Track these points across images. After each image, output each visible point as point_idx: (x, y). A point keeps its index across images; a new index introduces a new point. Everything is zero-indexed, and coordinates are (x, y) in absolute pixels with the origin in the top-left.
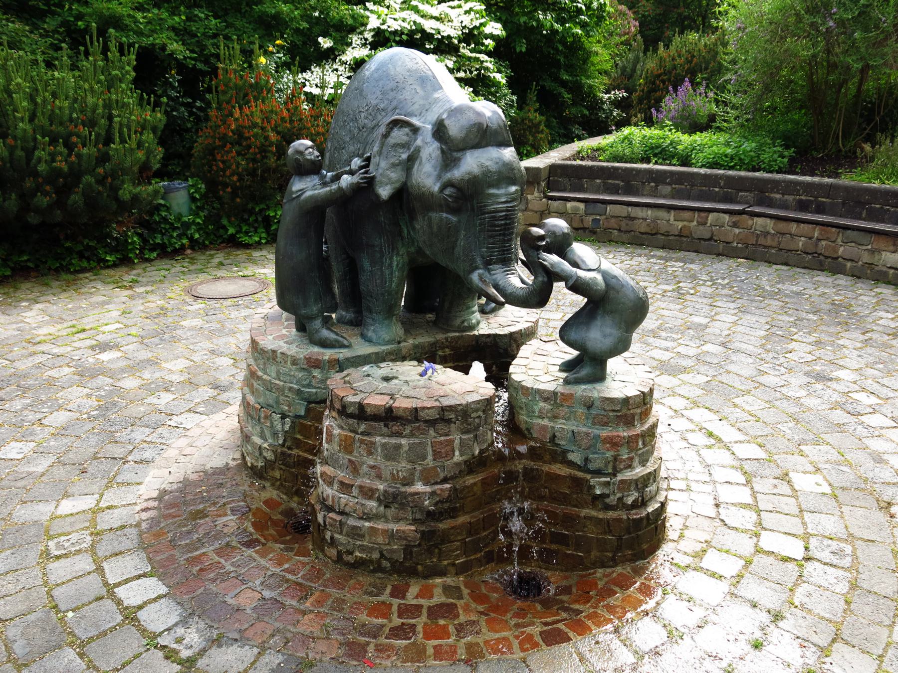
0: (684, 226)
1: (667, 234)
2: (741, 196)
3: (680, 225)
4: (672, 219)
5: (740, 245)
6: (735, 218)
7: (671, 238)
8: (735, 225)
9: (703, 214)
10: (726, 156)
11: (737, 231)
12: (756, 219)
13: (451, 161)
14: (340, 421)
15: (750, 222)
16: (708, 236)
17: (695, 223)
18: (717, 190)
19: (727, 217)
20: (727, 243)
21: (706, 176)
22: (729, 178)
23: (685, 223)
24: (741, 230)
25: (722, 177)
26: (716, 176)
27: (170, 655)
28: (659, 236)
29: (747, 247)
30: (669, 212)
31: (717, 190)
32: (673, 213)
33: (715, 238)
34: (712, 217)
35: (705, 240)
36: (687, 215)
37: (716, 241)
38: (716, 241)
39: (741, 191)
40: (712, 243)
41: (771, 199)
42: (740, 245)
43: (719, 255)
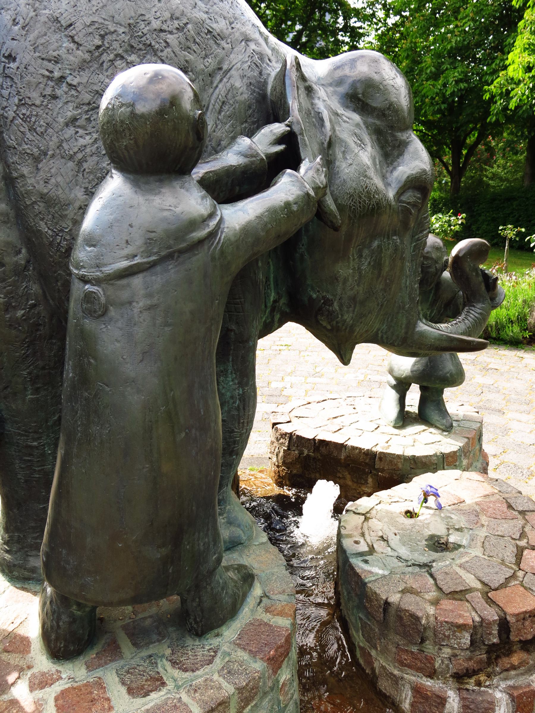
13: (394, 147)
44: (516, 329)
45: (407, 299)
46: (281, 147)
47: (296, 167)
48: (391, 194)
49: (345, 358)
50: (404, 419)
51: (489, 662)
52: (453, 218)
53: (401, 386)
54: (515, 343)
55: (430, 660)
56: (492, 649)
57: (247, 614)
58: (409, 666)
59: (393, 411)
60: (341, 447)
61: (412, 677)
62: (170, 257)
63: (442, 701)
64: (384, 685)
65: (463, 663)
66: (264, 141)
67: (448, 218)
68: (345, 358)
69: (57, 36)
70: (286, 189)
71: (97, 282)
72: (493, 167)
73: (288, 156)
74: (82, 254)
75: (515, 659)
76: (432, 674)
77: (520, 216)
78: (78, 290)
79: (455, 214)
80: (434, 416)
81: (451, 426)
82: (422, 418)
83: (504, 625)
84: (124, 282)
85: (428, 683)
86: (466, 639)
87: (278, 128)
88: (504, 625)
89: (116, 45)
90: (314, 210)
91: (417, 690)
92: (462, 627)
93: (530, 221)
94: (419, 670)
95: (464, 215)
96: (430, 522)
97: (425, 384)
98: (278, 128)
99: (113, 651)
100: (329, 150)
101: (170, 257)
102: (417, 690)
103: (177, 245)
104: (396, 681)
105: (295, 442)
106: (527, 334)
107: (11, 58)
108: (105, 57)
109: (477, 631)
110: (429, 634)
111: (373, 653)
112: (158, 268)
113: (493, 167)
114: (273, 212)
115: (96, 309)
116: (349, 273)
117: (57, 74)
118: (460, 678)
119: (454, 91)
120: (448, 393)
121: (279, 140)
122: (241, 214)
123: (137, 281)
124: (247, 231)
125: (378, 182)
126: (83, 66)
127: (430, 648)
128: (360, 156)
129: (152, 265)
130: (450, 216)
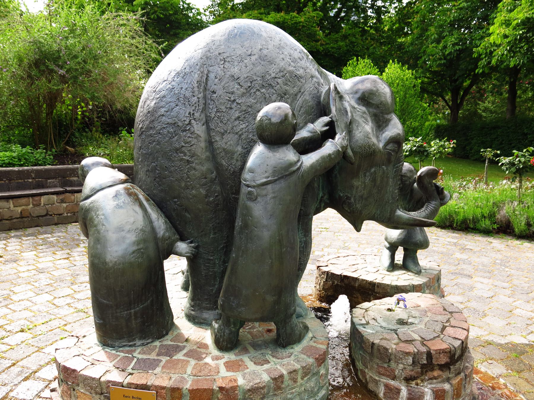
0: (23, 210)
1: (11, 219)
2: (50, 183)
3: (19, 209)
4: (12, 206)
5: (69, 214)
6: (61, 197)
7: (14, 221)
8: (62, 201)
9: (36, 198)
10: (14, 158)
11: (65, 205)
12: (76, 195)
13: (383, 122)
14: (445, 375)
15: (73, 197)
16: (44, 213)
17: (31, 206)
18: (30, 180)
19: (55, 197)
20: (60, 215)
21: (19, 171)
22: (37, 171)
23: (23, 207)
24: (67, 204)
25: (33, 171)
26: (28, 170)
28: (4, 221)
29: (74, 214)
30: (8, 202)
31: (30, 180)
32: (11, 201)
33: (50, 213)
34: (43, 199)
35: (42, 216)
36: (24, 201)
37: (51, 215)
38: (51, 215)
39: (49, 179)
40: (48, 217)
41: (71, 181)
42: (69, 214)
43: (56, 224)
44: (488, 222)
45: (390, 198)
46: (327, 128)
47: (333, 138)
48: (381, 145)
49: (358, 229)
50: (393, 267)
51: (422, 374)
53: (393, 248)
54: (487, 232)
55: (393, 371)
56: (423, 366)
57: (305, 342)
58: (383, 375)
59: (387, 262)
60: (356, 279)
61: (384, 380)
62: (282, 178)
63: (398, 391)
64: (371, 386)
65: (409, 372)
66: (319, 125)
68: (358, 229)
69: (233, 83)
70: (329, 148)
71: (254, 187)
72: (485, 103)
73: (330, 133)
74: (246, 176)
75: (436, 373)
76: (394, 378)
77: (503, 140)
78: (244, 190)
79: (448, 140)
80: (411, 265)
81: (420, 271)
82: (404, 267)
84: (264, 187)
85: (392, 382)
86: (410, 360)
87: (326, 119)
88: (429, 355)
89: (257, 85)
90: (342, 155)
91: (387, 386)
92: (408, 354)
93: (511, 144)
94: (388, 376)
95: (455, 141)
96: (400, 313)
98: (326, 119)
99: (245, 350)
100: (349, 128)
101: (282, 178)
102: (387, 386)
103: (285, 173)
104: (376, 382)
105: (330, 276)
106: (495, 226)
107: (214, 92)
108: (252, 91)
109: (416, 356)
110: (393, 357)
111: (366, 371)
112: (278, 182)
113: (485, 103)
114: (323, 158)
115: (252, 197)
116: (360, 184)
117: (232, 99)
118: (408, 380)
119: (451, 52)
120: (421, 254)
121: (326, 125)
122: (310, 159)
123: (269, 187)
124: (312, 166)
125: (374, 140)
126: (243, 95)
127: (393, 364)
128: (365, 128)
129: (275, 181)
130: (445, 142)
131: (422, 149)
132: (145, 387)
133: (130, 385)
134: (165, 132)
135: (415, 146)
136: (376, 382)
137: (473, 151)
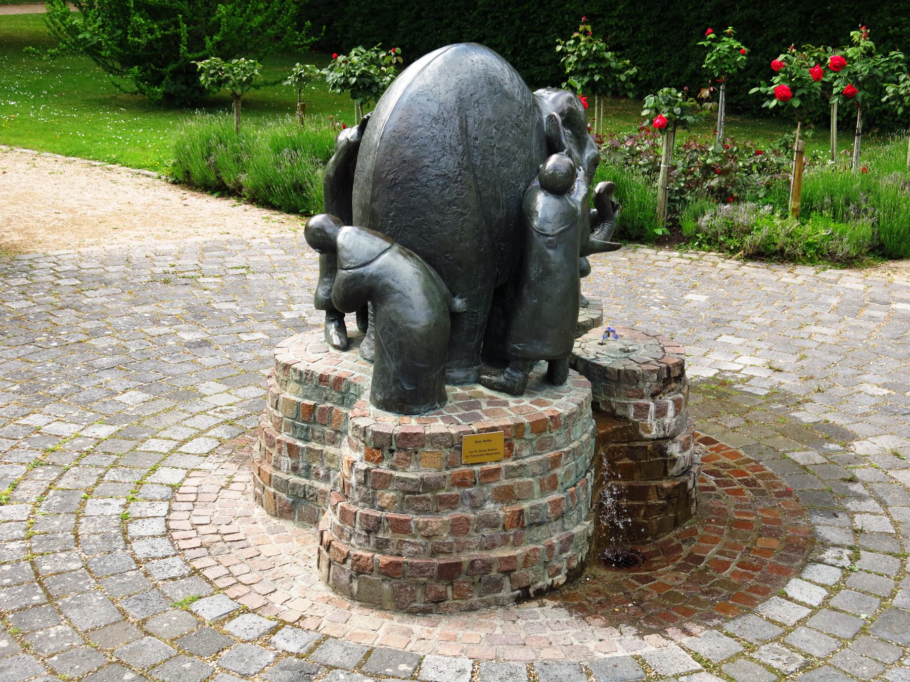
27: (855, 558)
51: (664, 387)
52: (382, 54)
55: (641, 390)
58: (631, 397)
61: (634, 401)
63: (648, 406)
64: (619, 412)
65: (654, 389)
67: (374, 55)
71: (553, 236)
75: (673, 385)
77: (422, 10)
81: (588, 304)
83: (668, 369)
85: (641, 401)
86: (655, 377)
88: (668, 369)
92: (653, 371)
93: (440, 19)
94: (637, 397)
97: (578, 274)
102: (637, 406)
104: (625, 406)
107: (476, 139)
109: (659, 372)
110: (641, 377)
111: (612, 399)
118: (653, 396)
127: (641, 384)
131: (367, 81)
132: (494, 429)
133: (479, 431)
134: (434, 184)
135: (353, 75)
136: (625, 406)
137: (350, 35)
